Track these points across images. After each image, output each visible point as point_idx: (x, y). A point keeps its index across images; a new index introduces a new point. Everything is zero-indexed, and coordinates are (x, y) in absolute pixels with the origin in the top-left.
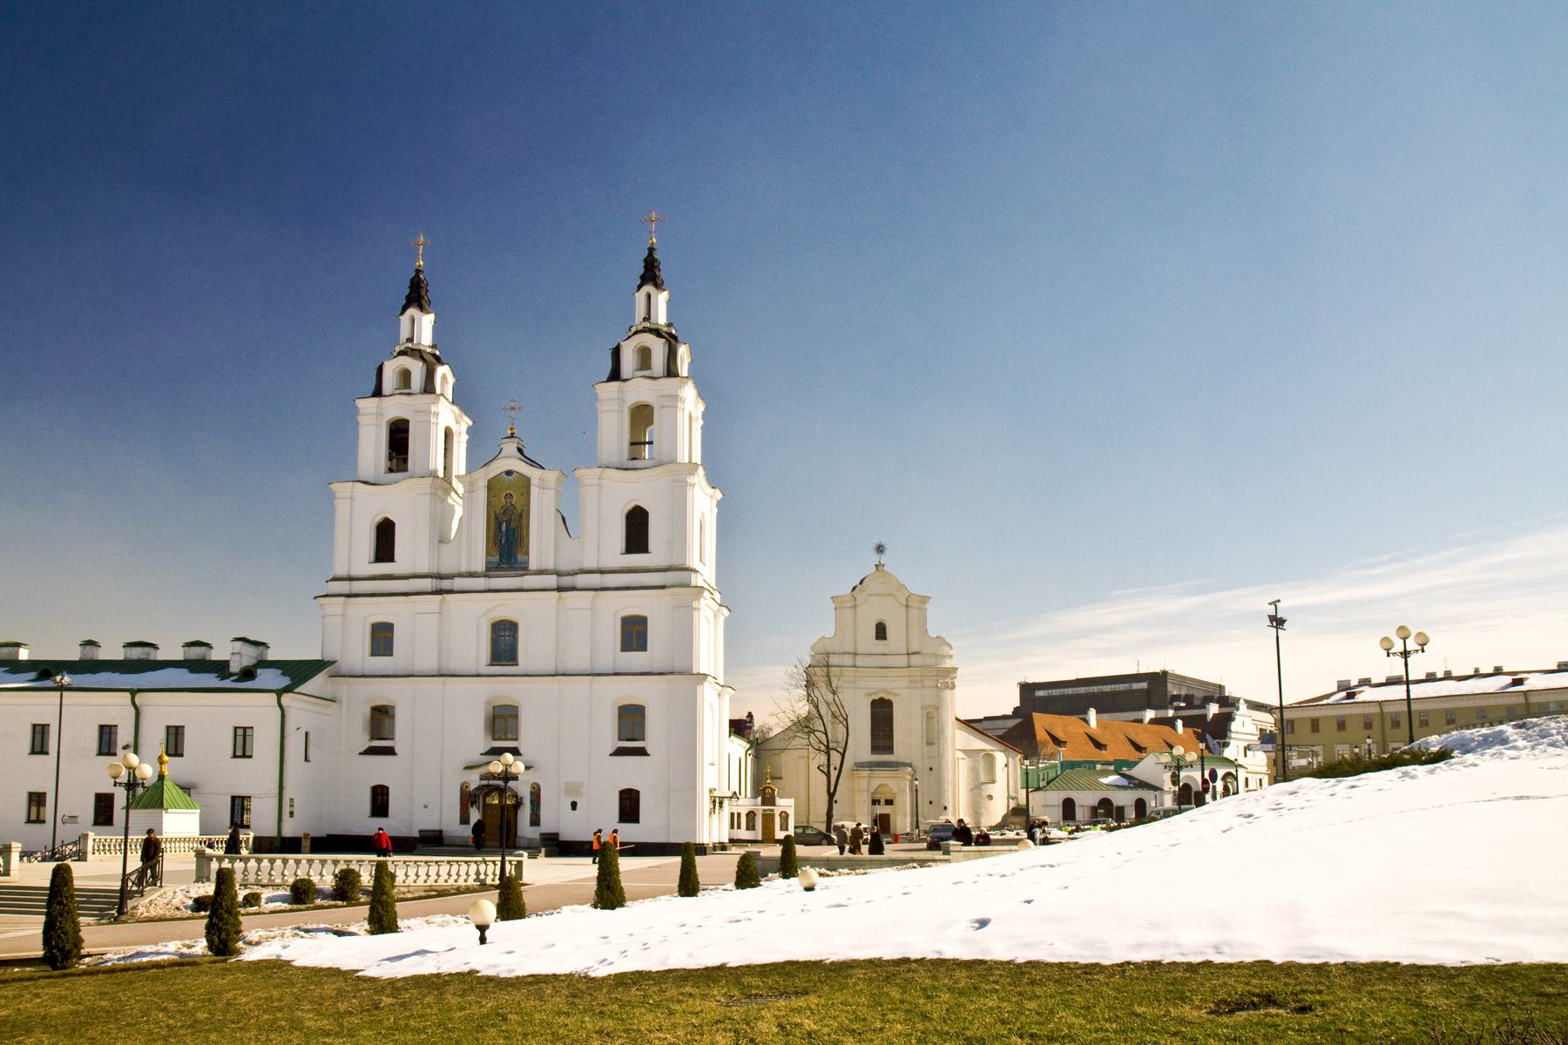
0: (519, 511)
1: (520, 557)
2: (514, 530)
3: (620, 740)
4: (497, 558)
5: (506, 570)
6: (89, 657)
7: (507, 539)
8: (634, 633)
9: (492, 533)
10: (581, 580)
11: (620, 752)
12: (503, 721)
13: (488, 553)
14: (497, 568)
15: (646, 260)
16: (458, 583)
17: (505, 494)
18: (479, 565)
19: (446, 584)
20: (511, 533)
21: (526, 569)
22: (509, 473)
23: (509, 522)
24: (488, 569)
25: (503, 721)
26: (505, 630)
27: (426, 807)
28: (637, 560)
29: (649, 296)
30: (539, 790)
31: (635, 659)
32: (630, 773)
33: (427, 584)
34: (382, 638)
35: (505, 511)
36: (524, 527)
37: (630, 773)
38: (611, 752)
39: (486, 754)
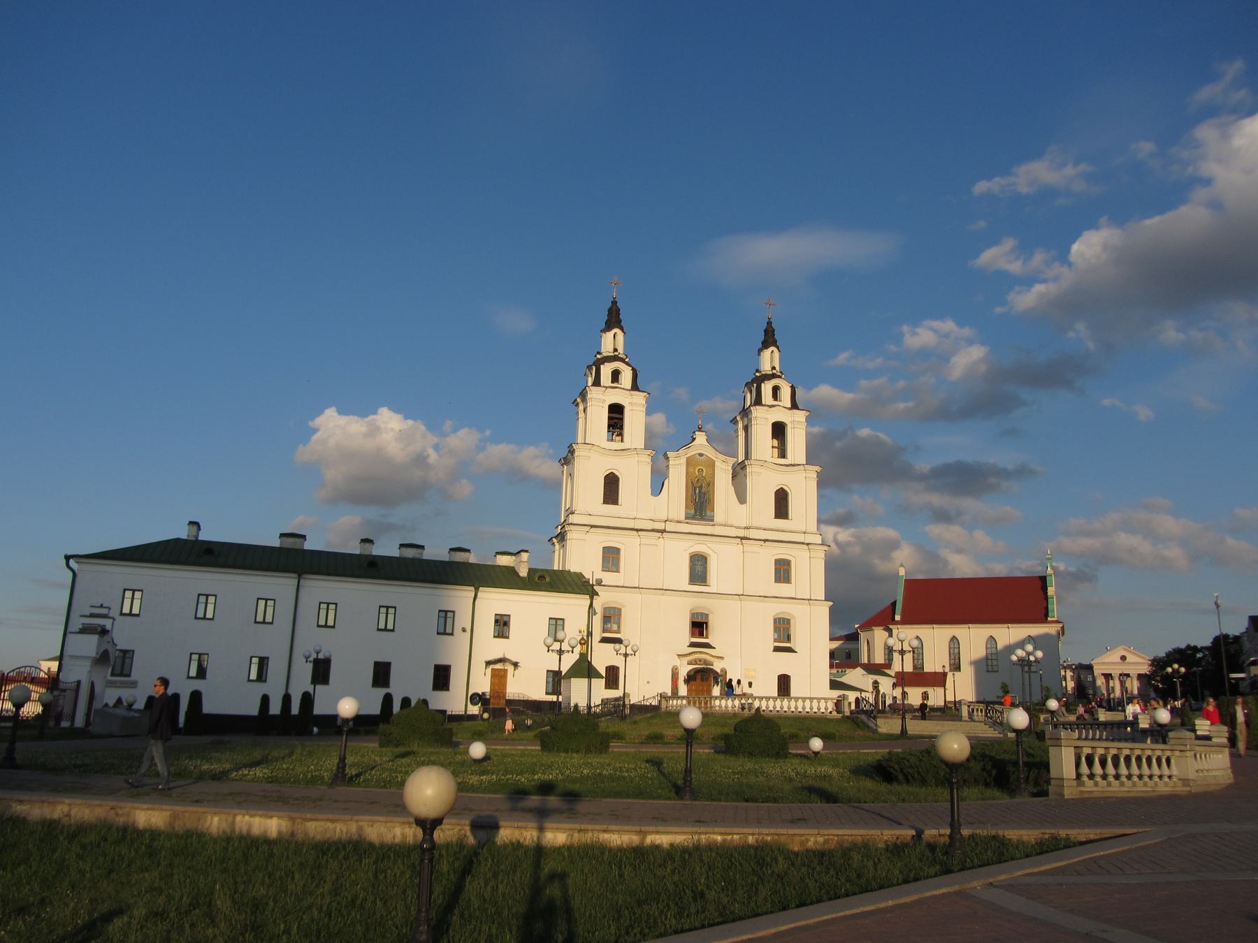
0: (708, 480)
1: (708, 513)
2: (705, 493)
3: (775, 641)
4: (693, 511)
5: (699, 520)
6: (367, 553)
7: (700, 497)
8: (783, 571)
9: (690, 494)
10: (753, 534)
11: (777, 649)
12: (699, 626)
13: (687, 507)
14: (693, 518)
15: (766, 331)
16: (670, 527)
17: (701, 467)
18: (682, 517)
19: (661, 526)
20: (702, 496)
21: (712, 520)
22: (701, 455)
23: (701, 487)
24: (686, 518)
25: (699, 626)
26: (698, 561)
27: (648, 682)
28: (781, 523)
29: (772, 352)
30: (726, 672)
31: (783, 590)
32: (784, 664)
33: (650, 525)
34: (611, 557)
35: (698, 480)
36: (711, 493)
37: (784, 664)
38: (772, 649)
39: (689, 646)
